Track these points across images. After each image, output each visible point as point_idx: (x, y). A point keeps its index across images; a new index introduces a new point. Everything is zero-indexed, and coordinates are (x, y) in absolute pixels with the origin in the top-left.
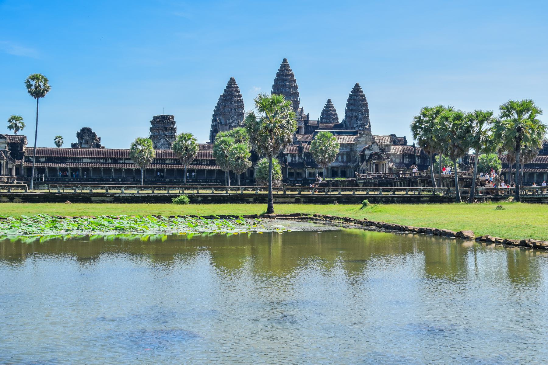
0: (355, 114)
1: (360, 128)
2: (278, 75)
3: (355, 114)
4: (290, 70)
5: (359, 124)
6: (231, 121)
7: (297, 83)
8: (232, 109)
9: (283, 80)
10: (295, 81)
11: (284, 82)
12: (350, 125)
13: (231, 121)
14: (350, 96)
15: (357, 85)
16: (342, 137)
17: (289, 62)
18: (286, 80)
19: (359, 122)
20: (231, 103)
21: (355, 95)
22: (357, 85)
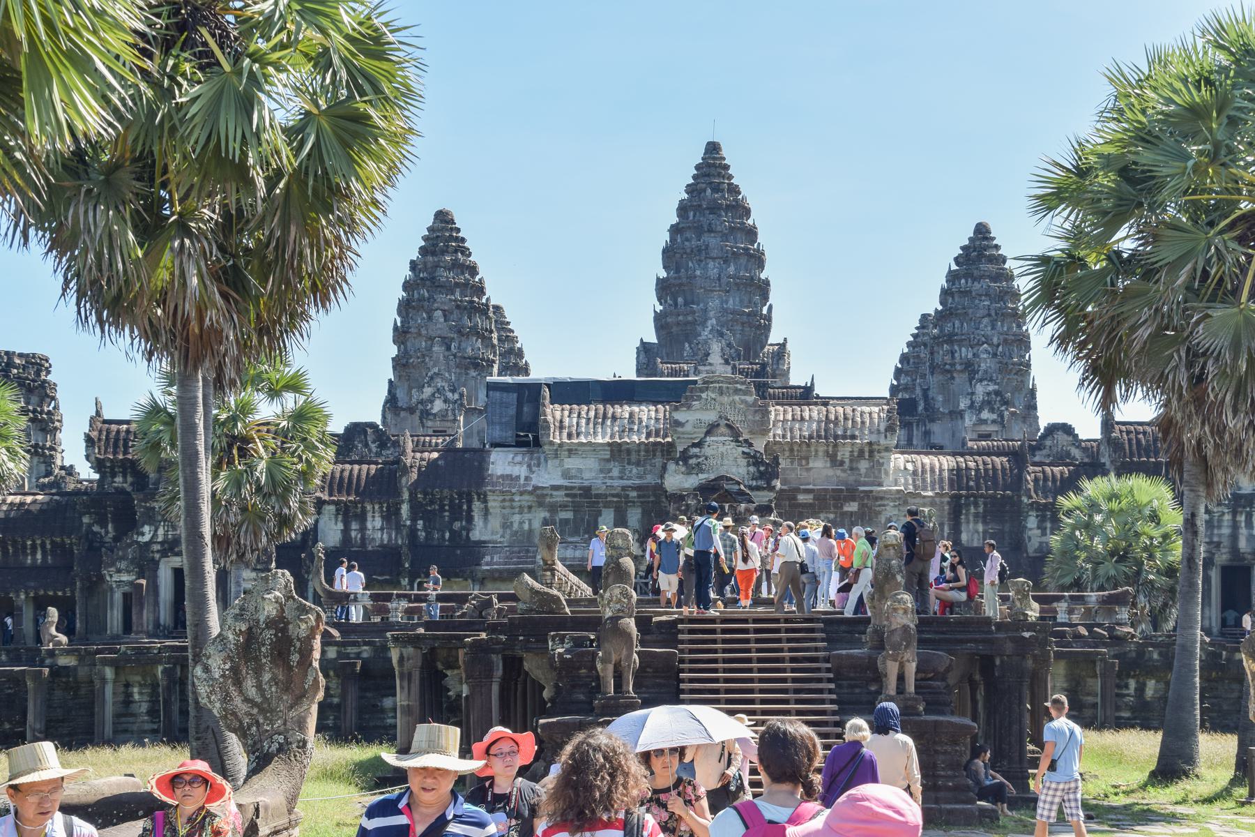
0: (965, 353)
1: (985, 415)
2: (683, 209)
3: (965, 353)
4: (735, 190)
5: (979, 397)
6: (428, 391)
7: (764, 240)
8: (432, 339)
9: (699, 230)
10: (751, 233)
11: (712, 239)
12: (946, 401)
13: (428, 391)
14: (952, 277)
15: (982, 231)
16: (624, 411)
17: (729, 154)
18: (710, 231)
19: (980, 390)
20: (430, 318)
21: (966, 276)
22: (982, 231)
